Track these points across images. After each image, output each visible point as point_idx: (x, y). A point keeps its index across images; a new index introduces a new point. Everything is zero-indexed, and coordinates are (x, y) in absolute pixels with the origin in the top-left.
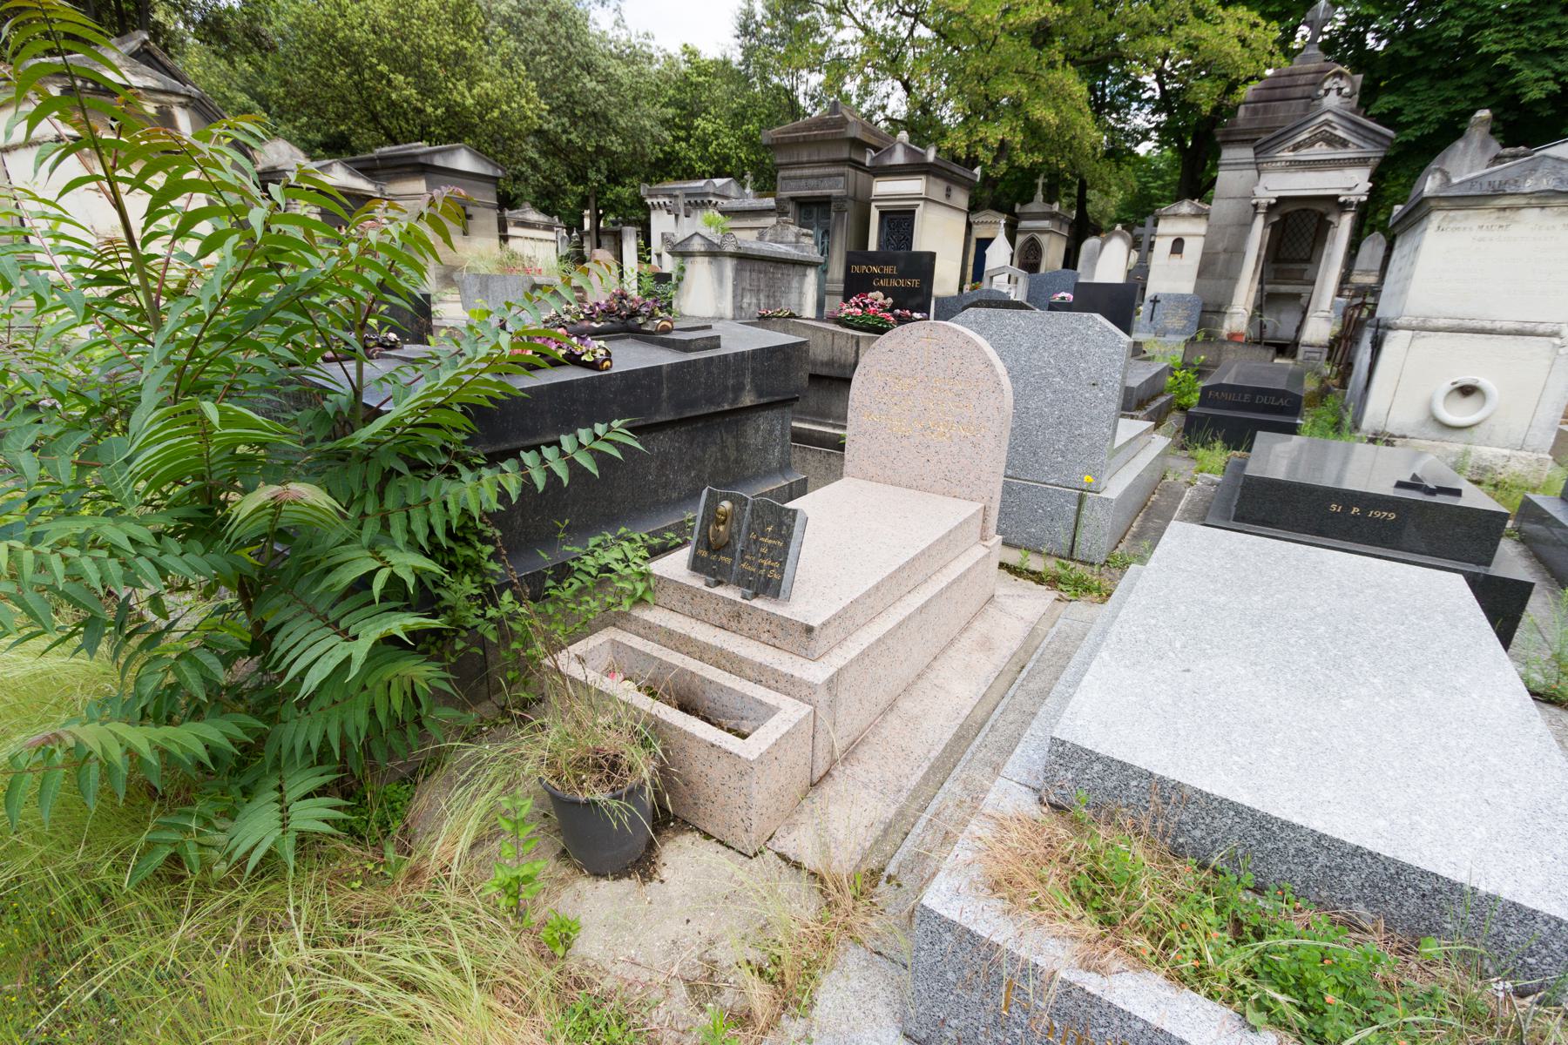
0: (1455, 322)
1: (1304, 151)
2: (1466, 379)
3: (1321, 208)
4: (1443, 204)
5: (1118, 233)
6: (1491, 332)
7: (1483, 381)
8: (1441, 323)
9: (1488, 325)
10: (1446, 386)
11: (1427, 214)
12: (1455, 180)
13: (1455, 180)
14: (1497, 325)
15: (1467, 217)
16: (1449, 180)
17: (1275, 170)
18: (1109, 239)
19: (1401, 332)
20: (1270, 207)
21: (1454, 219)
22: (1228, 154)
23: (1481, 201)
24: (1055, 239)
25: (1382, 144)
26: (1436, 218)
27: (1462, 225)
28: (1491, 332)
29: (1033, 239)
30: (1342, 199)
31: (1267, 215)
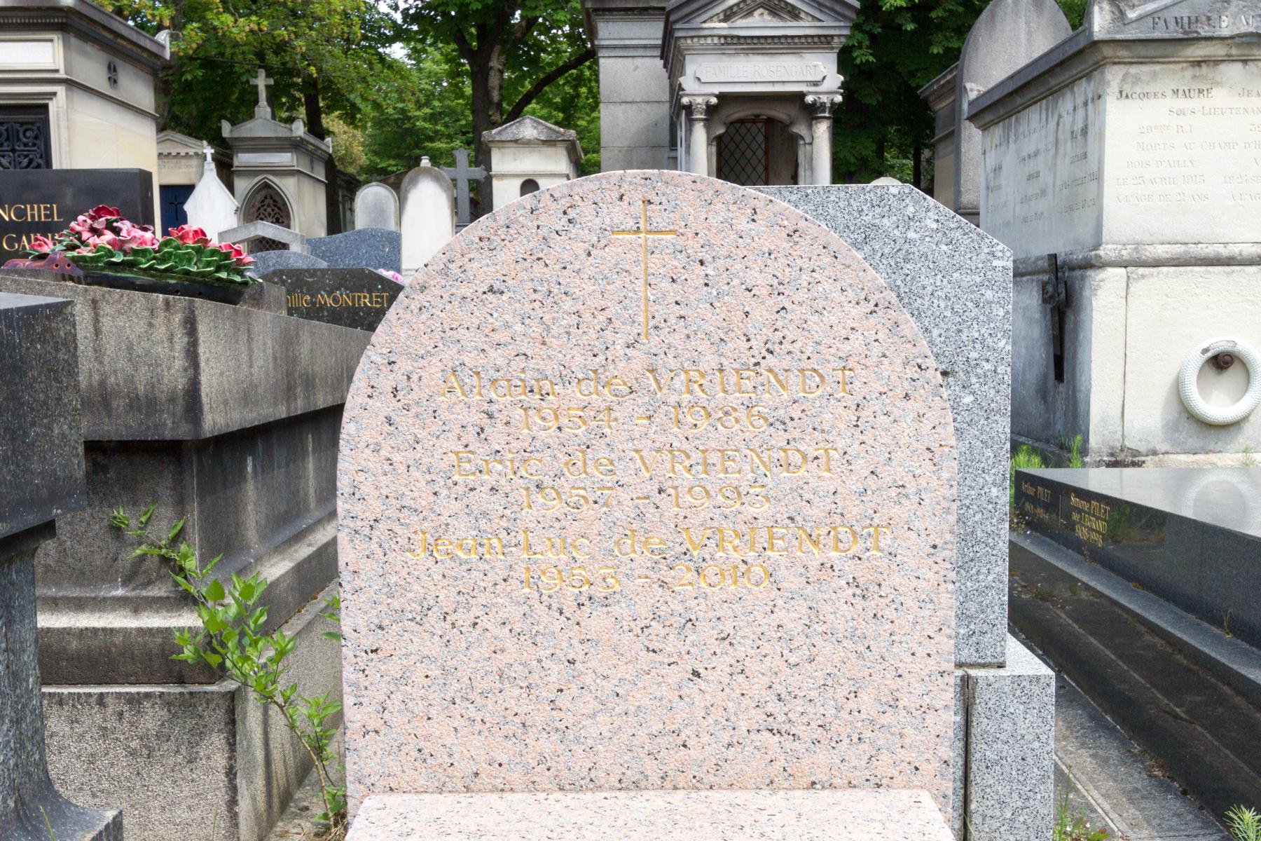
0: (1177, 250)
1: (741, 22)
2: (1219, 342)
3: (780, 113)
4: (1122, 53)
5: (426, 171)
6: (1229, 262)
7: (1244, 345)
8: (1162, 251)
9: (1224, 251)
10: (1196, 360)
11: (1099, 66)
12: (1132, 15)
13: (1132, 15)
14: (1234, 250)
15: (1154, 75)
16: (1122, 13)
17: (705, 51)
18: (414, 182)
19: (1111, 271)
20: (711, 110)
21: (1137, 80)
23: (1170, 49)
24: (307, 185)
25: (845, 17)
26: (1114, 76)
27: (1150, 89)
28: (1229, 262)
29: (266, 186)
30: (809, 99)
31: (708, 123)
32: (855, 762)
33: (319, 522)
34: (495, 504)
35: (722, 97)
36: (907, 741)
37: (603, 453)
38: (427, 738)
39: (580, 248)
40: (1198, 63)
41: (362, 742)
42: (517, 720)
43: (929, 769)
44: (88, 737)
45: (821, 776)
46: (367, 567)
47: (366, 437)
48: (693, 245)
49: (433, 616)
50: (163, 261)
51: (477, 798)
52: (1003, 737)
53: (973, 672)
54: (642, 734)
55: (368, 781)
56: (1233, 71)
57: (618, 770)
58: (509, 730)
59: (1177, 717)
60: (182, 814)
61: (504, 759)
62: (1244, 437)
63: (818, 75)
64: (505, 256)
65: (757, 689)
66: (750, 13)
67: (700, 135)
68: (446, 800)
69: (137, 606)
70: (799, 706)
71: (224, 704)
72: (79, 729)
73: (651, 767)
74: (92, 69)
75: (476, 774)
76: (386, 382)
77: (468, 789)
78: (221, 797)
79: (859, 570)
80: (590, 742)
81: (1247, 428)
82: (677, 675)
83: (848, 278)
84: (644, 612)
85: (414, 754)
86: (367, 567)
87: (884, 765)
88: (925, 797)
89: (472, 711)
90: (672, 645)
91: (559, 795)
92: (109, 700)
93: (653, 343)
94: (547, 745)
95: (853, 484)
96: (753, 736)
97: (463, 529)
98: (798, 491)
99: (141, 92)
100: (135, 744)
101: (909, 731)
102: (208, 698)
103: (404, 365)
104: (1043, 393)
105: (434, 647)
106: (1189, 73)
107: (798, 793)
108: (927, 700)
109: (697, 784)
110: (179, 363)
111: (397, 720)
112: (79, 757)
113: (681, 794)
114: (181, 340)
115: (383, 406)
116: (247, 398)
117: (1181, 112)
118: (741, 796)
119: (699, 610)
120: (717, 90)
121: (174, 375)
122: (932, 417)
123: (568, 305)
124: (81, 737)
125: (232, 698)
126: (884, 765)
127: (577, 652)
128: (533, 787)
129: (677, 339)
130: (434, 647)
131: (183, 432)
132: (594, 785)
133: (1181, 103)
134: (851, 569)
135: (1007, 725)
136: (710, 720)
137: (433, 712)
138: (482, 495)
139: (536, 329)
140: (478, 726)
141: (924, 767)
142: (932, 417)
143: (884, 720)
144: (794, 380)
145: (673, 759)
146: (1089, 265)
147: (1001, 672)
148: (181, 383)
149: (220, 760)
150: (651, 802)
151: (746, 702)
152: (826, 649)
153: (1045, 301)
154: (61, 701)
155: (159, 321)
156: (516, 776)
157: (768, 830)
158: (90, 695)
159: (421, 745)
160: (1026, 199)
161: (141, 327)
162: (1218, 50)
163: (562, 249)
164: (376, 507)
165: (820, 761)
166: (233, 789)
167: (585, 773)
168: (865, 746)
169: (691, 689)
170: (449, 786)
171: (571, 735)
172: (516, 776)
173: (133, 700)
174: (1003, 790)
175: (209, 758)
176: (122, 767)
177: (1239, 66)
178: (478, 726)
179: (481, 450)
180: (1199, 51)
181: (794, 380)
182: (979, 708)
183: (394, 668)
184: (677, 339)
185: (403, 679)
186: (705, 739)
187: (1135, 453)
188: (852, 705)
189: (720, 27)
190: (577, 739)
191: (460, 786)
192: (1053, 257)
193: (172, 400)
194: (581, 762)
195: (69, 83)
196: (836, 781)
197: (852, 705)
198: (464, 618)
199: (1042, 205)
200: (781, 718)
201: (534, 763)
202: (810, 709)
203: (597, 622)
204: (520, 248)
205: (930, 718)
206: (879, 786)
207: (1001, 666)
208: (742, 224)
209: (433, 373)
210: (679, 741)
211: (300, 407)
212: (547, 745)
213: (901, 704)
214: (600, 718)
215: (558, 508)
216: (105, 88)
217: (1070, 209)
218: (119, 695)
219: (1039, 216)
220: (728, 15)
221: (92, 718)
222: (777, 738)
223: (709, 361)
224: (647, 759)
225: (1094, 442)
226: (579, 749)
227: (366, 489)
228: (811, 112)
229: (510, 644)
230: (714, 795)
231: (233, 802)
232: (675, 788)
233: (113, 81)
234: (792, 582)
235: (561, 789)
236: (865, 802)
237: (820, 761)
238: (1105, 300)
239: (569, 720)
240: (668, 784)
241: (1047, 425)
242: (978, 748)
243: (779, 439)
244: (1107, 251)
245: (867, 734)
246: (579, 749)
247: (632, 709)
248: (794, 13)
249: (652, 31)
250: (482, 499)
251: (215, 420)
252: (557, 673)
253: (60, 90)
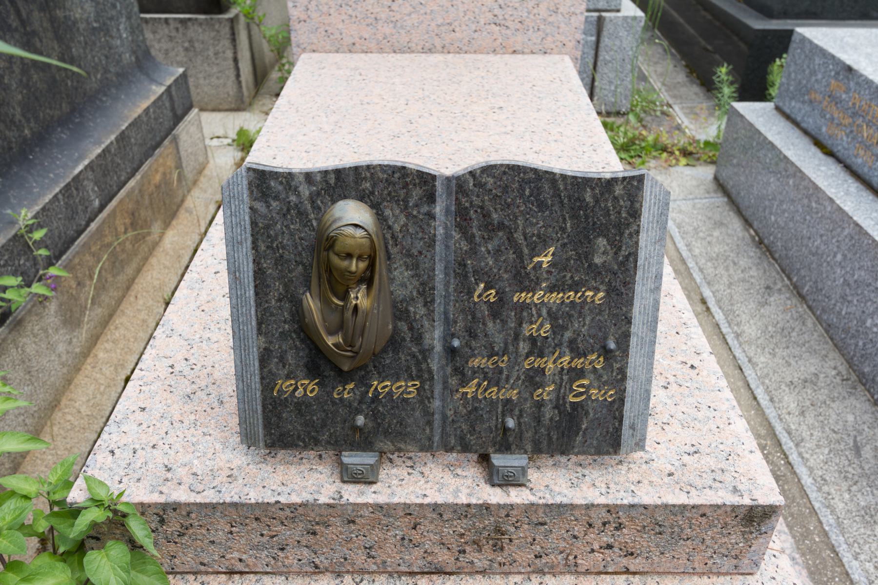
32: (535, 41)
36: (561, 30)
38: (329, 25)
41: (298, 26)
42: (373, 16)
43: (571, 45)
44: (163, 40)
45: (518, 47)
51: (355, 56)
52: (615, 48)
53: (604, 14)
54: (433, 24)
55: (303, 46)
57: (422, 43)
58: (370, 21)
59: (707, 50)
60: (214, 80)
61: (367, 36)
68: (339, 57)
70: (509, 11)
71: (228, 25)
72: (158, 37)
73: (438, 42)
75: (354, 44)
77: (350, 51)
78: (232, 73)
80: (408, 28)
85: (324, 33)
87: (549, 43)
88: (567, 59)
89: (350, 12)
91: (394, 55)
92: (171, 22)
94: (388, 29)
96: (487, 27)
100: (186, 45)
101: (562, 25)
102: (220, 21)
107: (507, 56)
108: (572, 9)
109: (459, 51)
111: (314, 15)
112: (160, 51)
113: (451, 55)
118: (480, 56)
124: (159, 41)
125: (233, 21)
126: (549, 43)
128: (381, 51)
132: (411, 51)
135: (618, 43)
136: (466, 18)
137: (332, 11)
140: (354, 19)
141: (568, 44)
143: (551, 19)
147: (619, 14)
149: (229, 54)
150: (437, 58)
151: (484, 8)
154: (146, 21)
157: (491, 70)
158: (160, 19)
159: (327, 28)
166: (237, 69)
167: (405, 44)
168: (540, 33)
170: (341, 50)
171: (399, 24)
172: (373, 45)
173: (183, 22)
174: (612, 75)
175: (224, 52)
176: (182, 56)
178: (354, 19)
182: (605, 33)
186: (464, 27)
188: (535, 11)
190: (402, 27)
191: (346, 49)
196: (526, 50)
197: (535, 11)
200: (501, 17)
201: (381, 38)
202: (515, 13)
205: (573, 19)
206: (545, 53)
207: (618, 11)
210: (451, 29)
212: (388, 29)
213: (559, 11)
214: (413, 16)
218: (175, 19)
221: (164, 31)
222: (498, 28)
224: (436, 38)
226: (403, 32)
230: (467, 56)
231: (238, 76)
232: (449, 53)
235: (395, 52)
236: (540, 59)
239: (398, 17)
240: (445, 51)
242: (603, 55)
245: (542, 27)
246: (403, 32)
247: (428, 11)
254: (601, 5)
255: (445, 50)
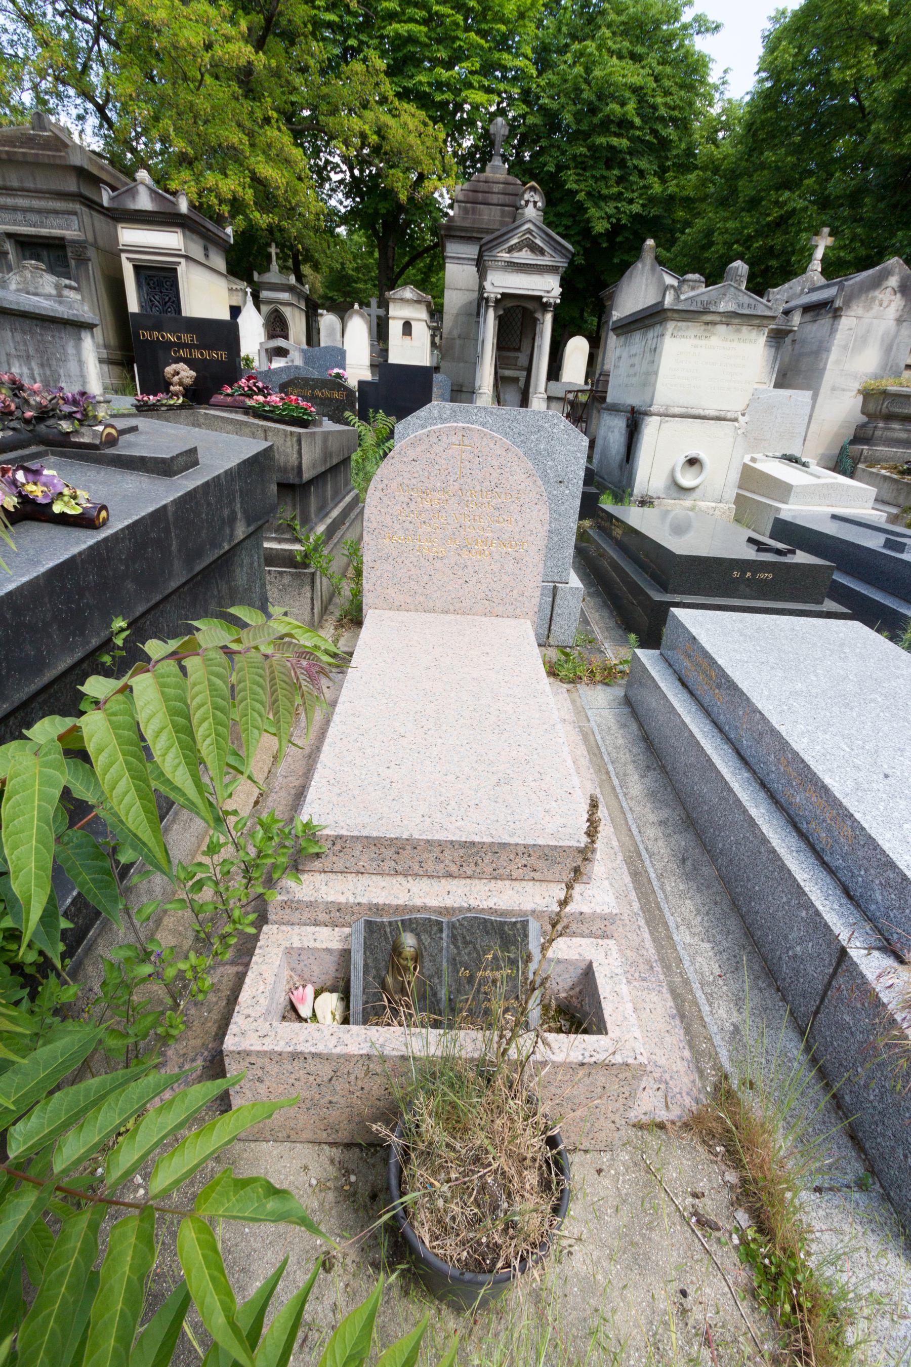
1: (516, 254)
3: (530, 305)
4: (676, 315)
15: (688, 327)
21: (680, 329)
22: (452, 249)
23: (697, 315)
27: (685, 334)
30: (545, 300)
33: (332, 509)
34: (411, 527)
35: (504, 295)
37: (444, 514)
39: (441, 449)
40: (707, 324)
43: (531, 614)
46: (371, 542)
47: (374, 503)
48: (476, 451)
49: (391, 559)
50: (284, 410)
56: (722, 329)
62: (695, 495)
63: (549, 287)
64: (418, 449)
65: (484, 587)
66: (521, 250)
67: (491, 314)
68: (392, 612)
69: (280, 541)
70: (495, 593)
74: (197, 251)
76: (380, 486)
78: (309, 607)
79: (516, 555)
81: (697, 490)
82: (461, 581)
83: (522, 465)
84: (453, 562)
86: (371, 542)
87: (518, 612)
88: (529, 622)
90: (460, 573)
93: (461, 481)
94: (422, 599)
95: (517, 529)
97: (401, 534)
98: (501, 530)
99: (220, 263)
102: (305, 574)
103: (386, 482)
104: (621, 467)
105: (390, 568)
106: (703, 328)
109: (464, 613)
110: (295, 456)
111: (379, 588)
114: (296, 447)
115: (379, 494)
116: (314, 466)
117: (696, 346)
119: (469, 563)
120: (501, 291)
121: (293, 459)
122: (543, 511)
123: (437, 467)
125: (313, 575)
126: (518, 612)
127: (432, 573)
128: (417, 610)
129: (469, 480)
130: (390, 568)
131: (296, 481)
132: (434, 611)
133: (697, 342)
134: (514, 554)
138: (407, 524)
139: (426, 474)
142: (543, 511)
144: (503, 496)
145: (458, 606)
146: (647, 414)
148: (296, 463)
152: (505, 577)
153: (628, 426)
155: (288, 439)
156: (412, 607)
160: (628, 376)
161: (282, 441)
162: (717, 318)
163: (437, 449)
164: (375, 525)
165: (500, 609)
169: (465, 586)
172: (412, 607)
177: (724, 326)
179: (408, 510)
180: (709, 318)
181: (503, 496)
182: (558, 597)
183: (378, 573)
184: (469, 480)
185: (381, 577)
187: (651, 498)
189: (505, 256)
192: (633, 408)
193: (293, 469)
194: (431, 605)
195: (187, 257)
198: (399, 560)
199: (634, 380)
203: (438, 564)
204: (423, 447)
208: (492, 446)
209: (394, 485)
211: (328, 466)
212: (422, 599)
215: (429, 529)
216: (202, 259)
217: (644, 385)
219: (632, 385)
220: (510, 250)
223: (478, 488)
225: (636, 491)
227: (372, 519)
228: (545, 307)
229: (413, 569)
231: (313, 609)
233: (207, 256)
234: (496, 556)
236: (512, 622)
237: (500, 609)
238: (650, 429)
241: (620, 482)
243: (497, 513)
244: (654, 409)
248: (542, 252)
249: (472, 251)
250: (407, 524)
251: (307, 476)
252: (426, 578)
253: (182, 260)
254: (556, 579)
255: (455, 612)
